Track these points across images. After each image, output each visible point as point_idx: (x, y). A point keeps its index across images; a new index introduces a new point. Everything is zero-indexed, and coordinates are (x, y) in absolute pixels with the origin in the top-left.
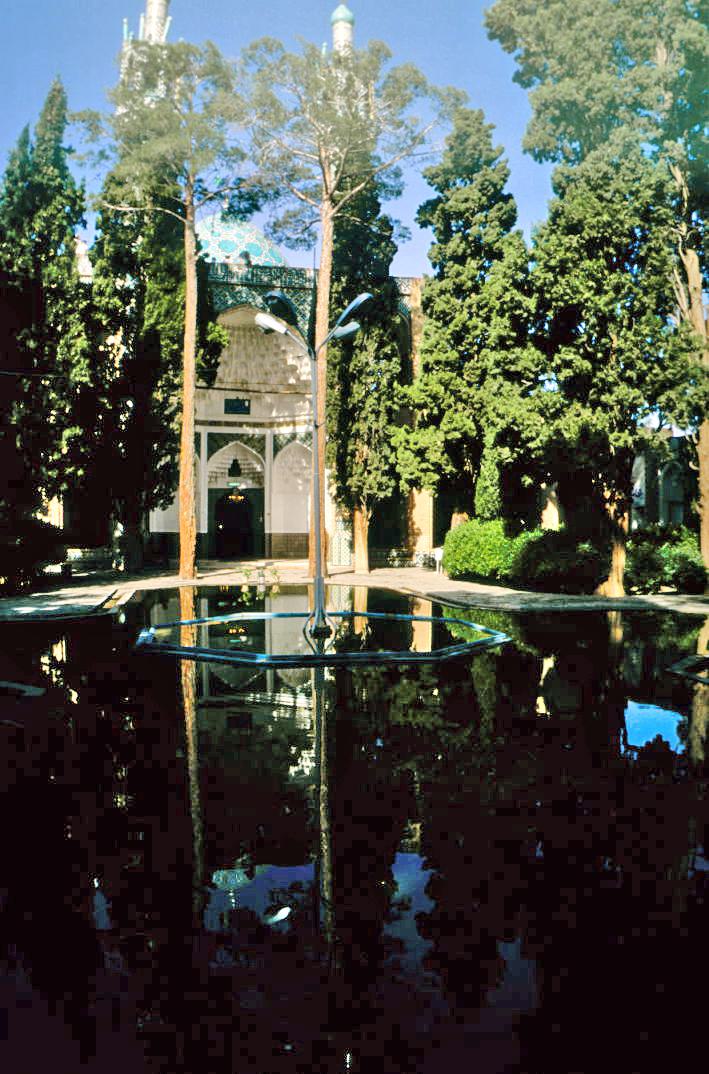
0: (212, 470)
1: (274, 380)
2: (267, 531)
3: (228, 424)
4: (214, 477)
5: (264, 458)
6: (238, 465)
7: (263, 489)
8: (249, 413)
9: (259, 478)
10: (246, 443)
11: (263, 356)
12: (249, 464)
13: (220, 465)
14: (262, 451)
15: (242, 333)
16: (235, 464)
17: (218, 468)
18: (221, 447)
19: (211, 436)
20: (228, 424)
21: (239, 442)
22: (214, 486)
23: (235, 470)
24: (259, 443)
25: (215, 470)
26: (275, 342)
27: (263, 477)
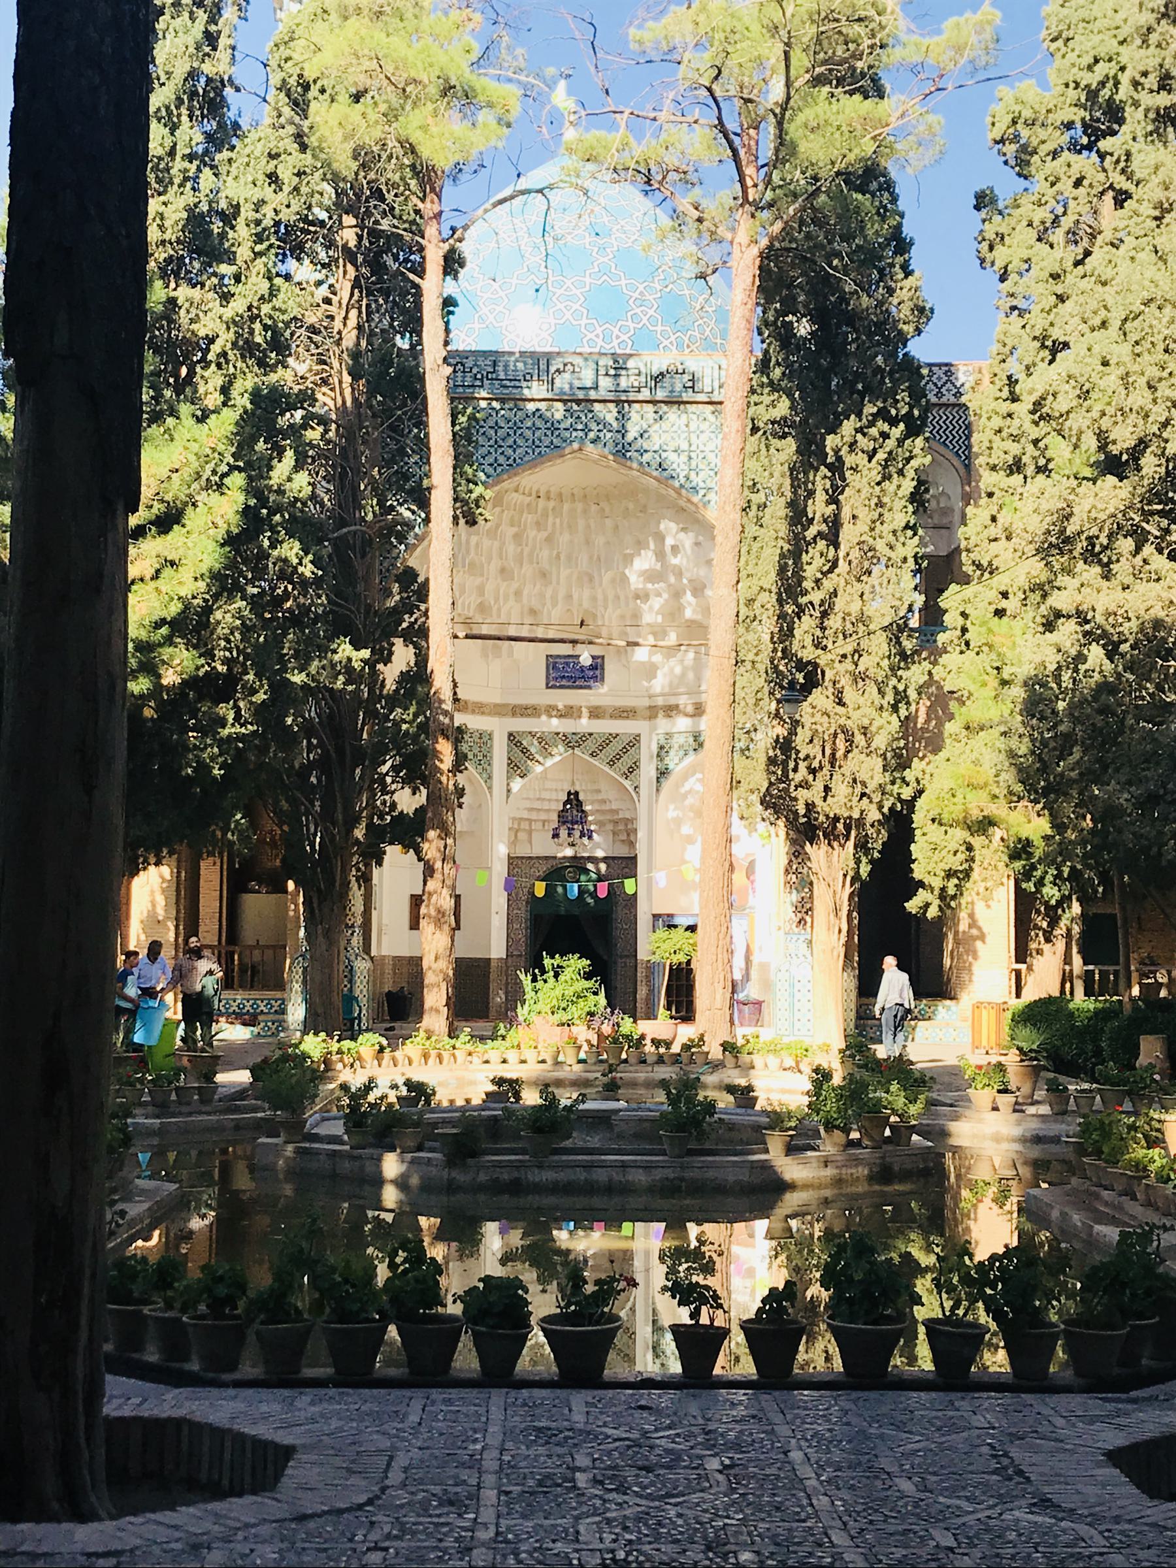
2: (642, 955)
6: (579, 804)
7: (635, 858)
9: (626, 830)
13: (537, 805)
15: (579, 506)
16: (573, 800)
17: (531, 810)
22: (523, 851)
23: (572, 812)
25: (525, 815)
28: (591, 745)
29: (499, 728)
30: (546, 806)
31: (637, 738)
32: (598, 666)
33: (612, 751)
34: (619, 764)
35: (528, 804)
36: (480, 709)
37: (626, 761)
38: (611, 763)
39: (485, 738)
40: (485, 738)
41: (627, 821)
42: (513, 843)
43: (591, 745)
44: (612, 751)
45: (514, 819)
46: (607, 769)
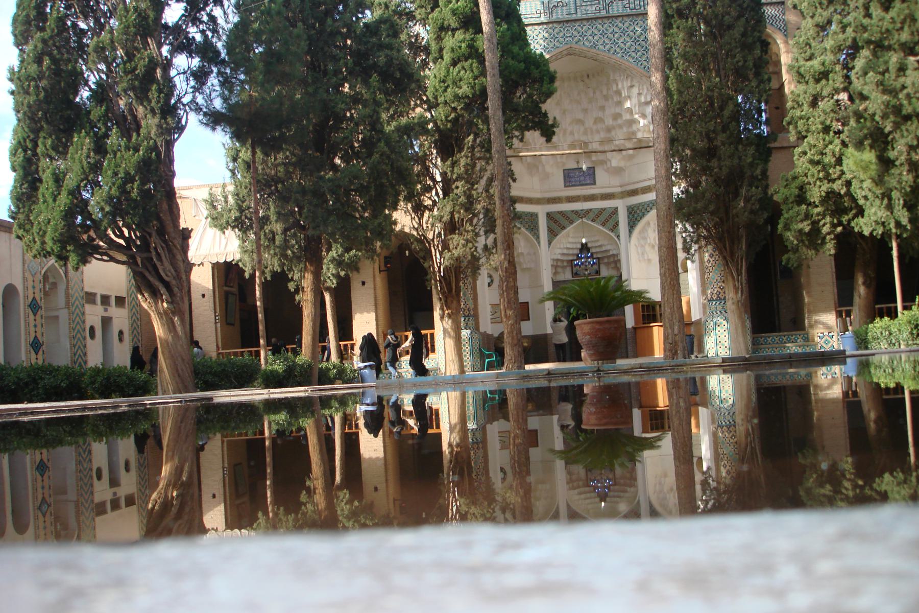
0: (556, 257)
1: (619, 136)
3: (570, 199)
4: (556, 266)
5: (618, 237)
8: (595, 183)
10: (593, 220)
11: (602, 108)
12: (601, 246)
13: (565, 251)
14: (615, 227)
17: (563, 254)
18: (564, 228)
19: (549, 215)
20: (570, 199)
21: (584, 220)
24: (608, 219)
25: (559, 257)
26: (614, 88)
27: (619, 260)
28: (591, 215)
29: (541, 211)
30: (571, 252)
31: (615, 211)
32: (592, 171)
33: (603, 218)
34: (607, 224)
35: (559, 251)
36: (530, 201)
37: (611, 223)
38: (603, 224)
39: (534, 217)
40: (534, 217)
41: (614, 255)
42: (555, 273)
43: (591, 215)
44: (603, 218)
45: (553, 260)
46: (601, 228)
